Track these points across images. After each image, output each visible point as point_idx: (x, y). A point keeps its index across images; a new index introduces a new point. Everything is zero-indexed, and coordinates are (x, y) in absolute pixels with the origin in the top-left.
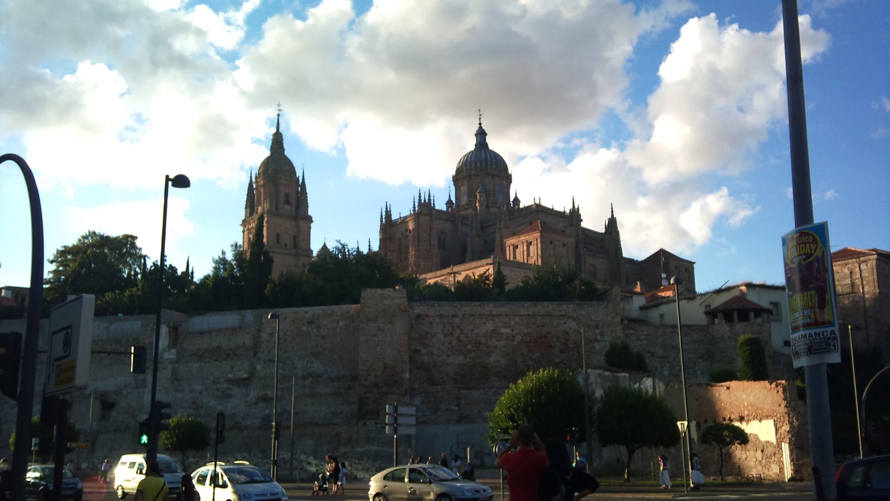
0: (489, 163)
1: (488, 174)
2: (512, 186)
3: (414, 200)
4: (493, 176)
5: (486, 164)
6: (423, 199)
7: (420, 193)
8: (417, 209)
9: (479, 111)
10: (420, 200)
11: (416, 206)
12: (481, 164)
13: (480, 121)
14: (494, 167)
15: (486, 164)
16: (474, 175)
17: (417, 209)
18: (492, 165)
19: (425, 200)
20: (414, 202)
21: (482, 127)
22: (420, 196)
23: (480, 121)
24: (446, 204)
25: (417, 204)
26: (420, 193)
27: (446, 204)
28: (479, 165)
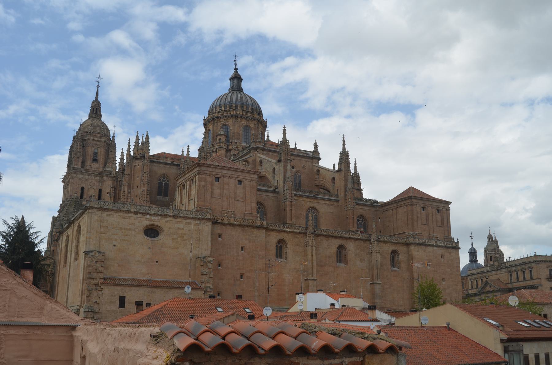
0: (234, 105)
1: (232, 116)
2: (267, 129)
3: (129, 143)
4: (236, 117)
5: (231, 106)
6: (140, 142)
7: (137, 136)
8: (132, 153)
9: (236, 56)
10: (137, 143)
11: (131, 150)
12: (225, 107)
13: (236, 66)
14: (239, 108)
15: (231, 106)
16: (218, 118)
17: (132, 153)
18: (236, 107)
19: (142, 143)
20: (129, 145)
21: (237, 72)
22: (137, 139)
23: (236, 66)
24: (198, 150)
25: (132, 148)
26: (137, 136)
27: (198, 150)
28: (223, 109)
